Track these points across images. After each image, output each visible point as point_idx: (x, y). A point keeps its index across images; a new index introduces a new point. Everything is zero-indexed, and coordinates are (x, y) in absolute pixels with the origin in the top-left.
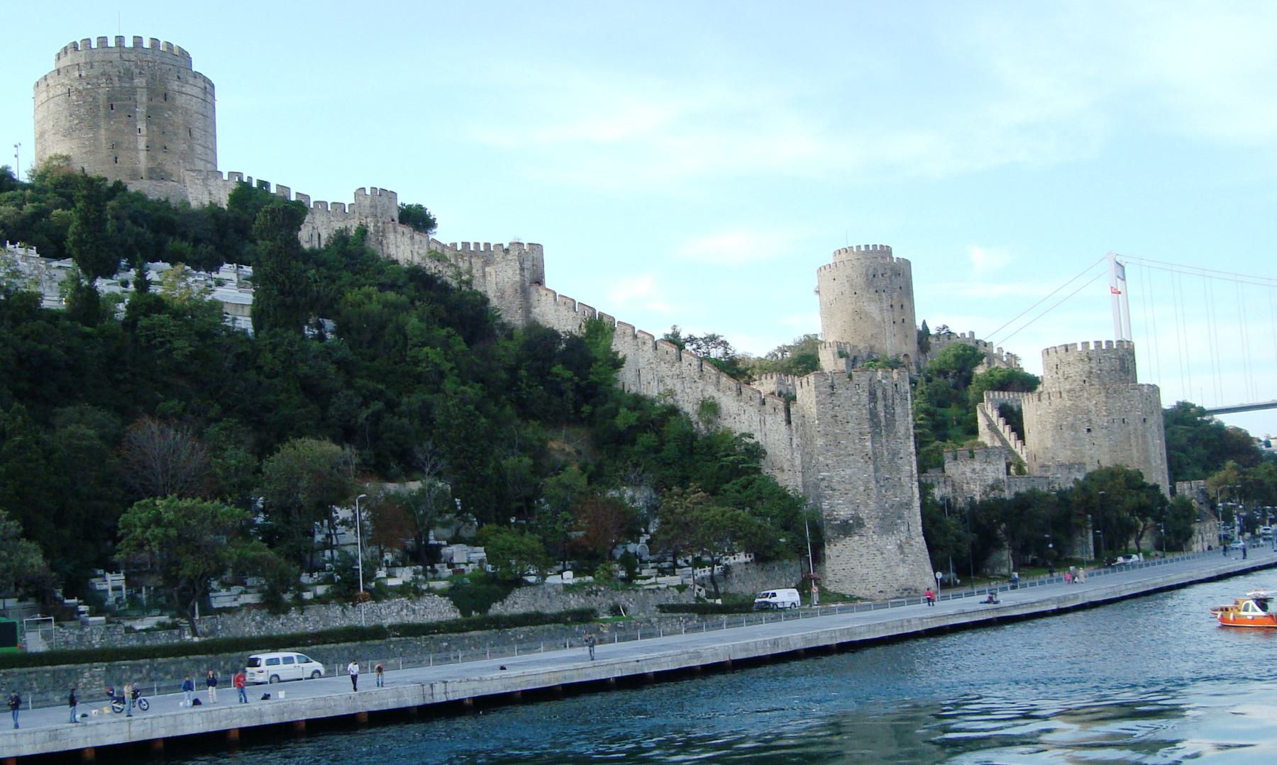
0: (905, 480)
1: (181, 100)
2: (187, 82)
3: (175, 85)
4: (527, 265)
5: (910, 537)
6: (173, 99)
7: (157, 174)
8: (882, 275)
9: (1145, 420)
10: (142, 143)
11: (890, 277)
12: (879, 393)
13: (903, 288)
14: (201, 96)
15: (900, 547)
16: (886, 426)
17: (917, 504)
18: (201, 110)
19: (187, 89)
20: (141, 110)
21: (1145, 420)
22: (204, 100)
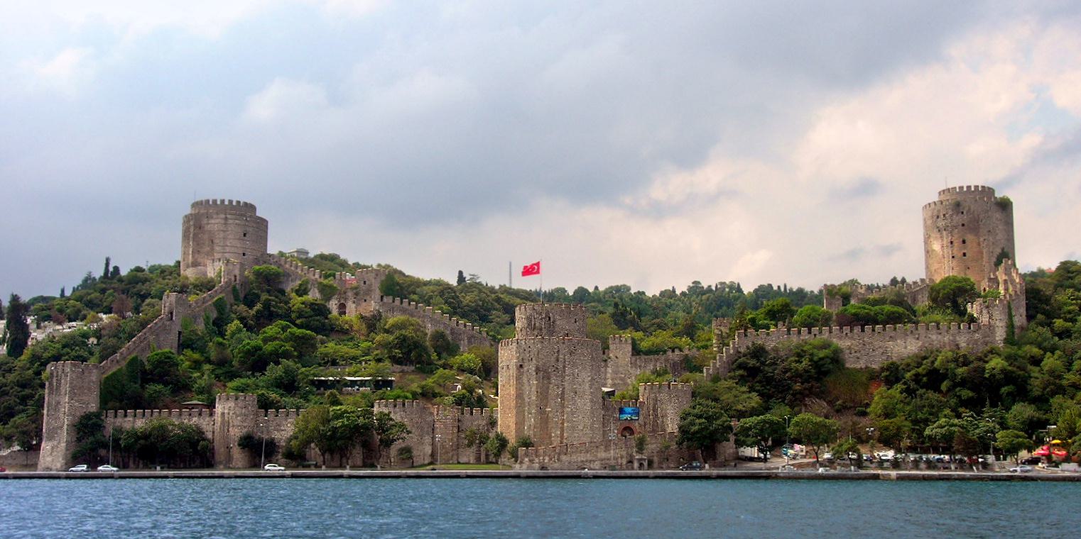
0: (61, 415)
1: (208, 227)
2: (212, 218)
3: (205, 221)
4: (167, 304)
5: (59, 443)
6: (204, 227)
7: (195, 264)
8: (944, 215)
9: (521, 366)
10: (191, 252)
11: (952, 216)
12: (55, 374)
13: (966, 224)
14: (223, 222)
15: (53, 448)
16: (56, 389)
17: (65, 427)
18: (222, 229)
19: (213, 221)
20: (191, 235)
21: (521, 366)
22: (225, 224)
